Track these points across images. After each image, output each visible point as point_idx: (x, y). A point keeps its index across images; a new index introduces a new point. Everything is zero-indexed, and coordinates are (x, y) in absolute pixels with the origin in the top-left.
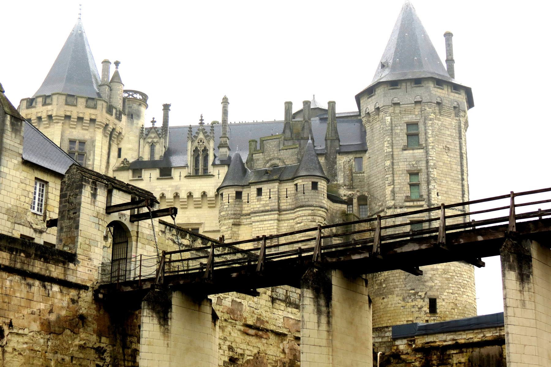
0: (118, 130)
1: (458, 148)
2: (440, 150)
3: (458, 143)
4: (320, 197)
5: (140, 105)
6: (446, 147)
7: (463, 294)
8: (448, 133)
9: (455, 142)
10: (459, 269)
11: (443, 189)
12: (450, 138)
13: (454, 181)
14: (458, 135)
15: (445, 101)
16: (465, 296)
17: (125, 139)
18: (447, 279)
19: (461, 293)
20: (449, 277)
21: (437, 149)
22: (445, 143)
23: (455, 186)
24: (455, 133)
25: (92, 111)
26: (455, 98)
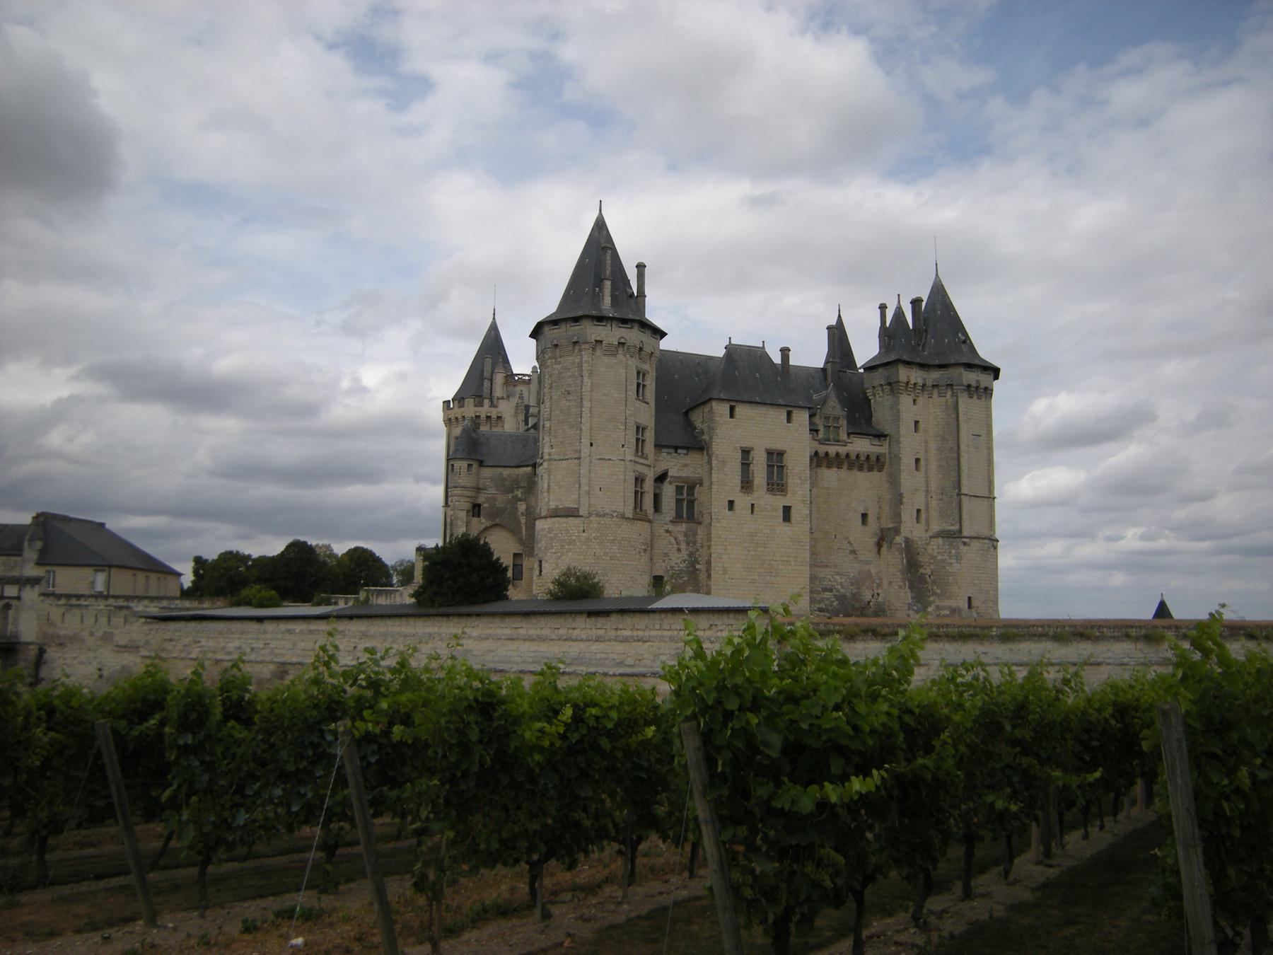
0: (494, 416)
1: (579, 388)
2: (557, 397)
3: (580, 381)
4: (455, 478)
5: (515, 386)
6: (566, 391)
8: (569, 374)
10: (565, 525)
15: (562, 341)
16: (570, 554)
17: (506, 420)
18: (551, 538)
19: (565, 550)
21: (554, 397)
25: (462, 410)
26: (574, 333)
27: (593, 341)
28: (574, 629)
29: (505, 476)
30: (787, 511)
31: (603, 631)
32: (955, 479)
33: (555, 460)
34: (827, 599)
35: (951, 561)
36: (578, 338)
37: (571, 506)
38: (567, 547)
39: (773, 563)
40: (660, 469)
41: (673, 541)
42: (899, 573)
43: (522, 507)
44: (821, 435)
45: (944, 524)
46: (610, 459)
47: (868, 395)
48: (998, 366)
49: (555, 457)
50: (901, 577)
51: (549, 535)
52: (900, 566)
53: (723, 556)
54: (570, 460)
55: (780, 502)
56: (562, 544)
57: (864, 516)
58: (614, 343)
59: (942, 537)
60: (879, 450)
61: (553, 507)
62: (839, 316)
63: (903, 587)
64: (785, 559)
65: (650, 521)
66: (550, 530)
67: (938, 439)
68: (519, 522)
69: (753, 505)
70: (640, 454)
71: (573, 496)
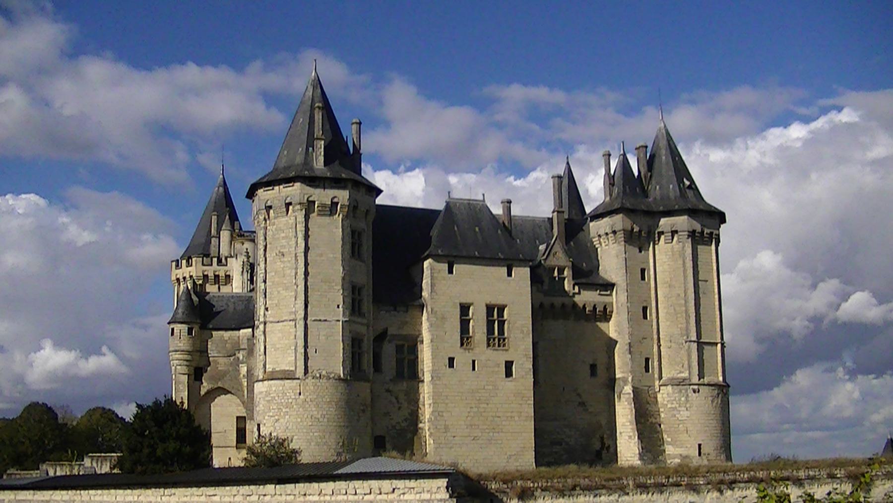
0: (222, 274)
4: (176, 342)
6: (280, 252)
7: (285, 415)
8: (283, 235)
9: (290, 243)
11: (273, 302)
12: (284, 241)
13: (287, 289)
14: (294, 234)
16: (287, 417)
18: (268, 401)
19: (282, 414)
20: (270, 399)
22: (279, 248)
23: (287, 294)
24: (292, 234)
25: (189, 268)
27: (305, 201)
28: (265, 495)
29: (226, 339)
30: (509, 365)
31: (292, 497)
32: (684, 325)
33: (272, 322)
34: (556, 453)
35: (680, 409)
36: (291, 199)
37: (287, 368)
38: (284, 410)
39: (496, 419)
40: (380, 329)
41: (394, 400)
42: (629, 424)
43: (244, 369)
44: (546, 287)
45: (673, 372)
46: (325, 320)
47: (595, 243)
48: (722, 210)
49: (271, 319)
50: (631, 427)
51: (267, 399)
52: (629, 417)
53: (444, 414)
54: (285, 323)
55: (501, 357)
56: (279, 407)
57: (593, 367)
58: (327, 203)
59: (672, 385)
60: (606, 299)
61: (271, 370)
62: (568, 163)
63: (633, 437)
64: (509, 414)
65: (368, 380)
66: (268, 393)
67: (665, 285)
68: (241, 384)
69: (474, 362)
70: (357, 313)
71: (289, 359)
